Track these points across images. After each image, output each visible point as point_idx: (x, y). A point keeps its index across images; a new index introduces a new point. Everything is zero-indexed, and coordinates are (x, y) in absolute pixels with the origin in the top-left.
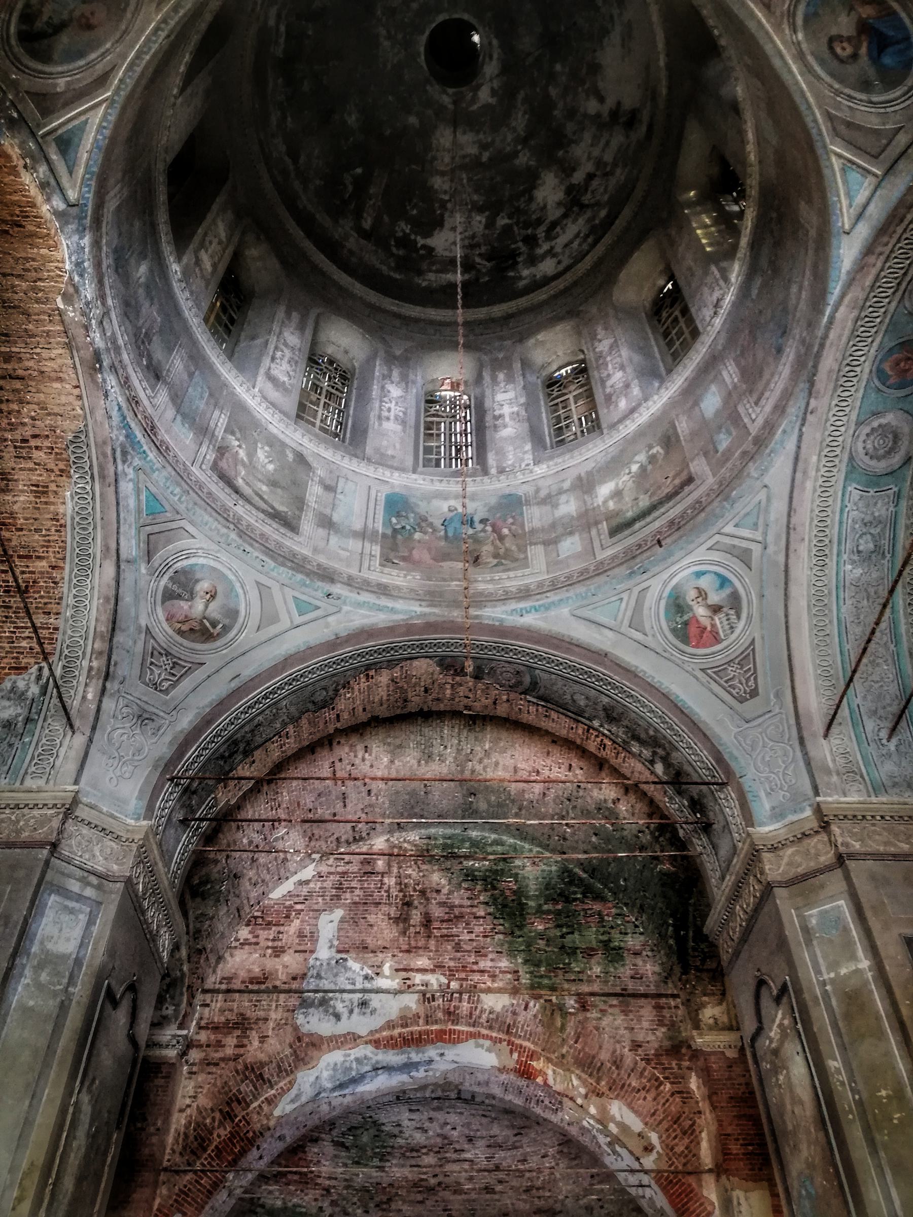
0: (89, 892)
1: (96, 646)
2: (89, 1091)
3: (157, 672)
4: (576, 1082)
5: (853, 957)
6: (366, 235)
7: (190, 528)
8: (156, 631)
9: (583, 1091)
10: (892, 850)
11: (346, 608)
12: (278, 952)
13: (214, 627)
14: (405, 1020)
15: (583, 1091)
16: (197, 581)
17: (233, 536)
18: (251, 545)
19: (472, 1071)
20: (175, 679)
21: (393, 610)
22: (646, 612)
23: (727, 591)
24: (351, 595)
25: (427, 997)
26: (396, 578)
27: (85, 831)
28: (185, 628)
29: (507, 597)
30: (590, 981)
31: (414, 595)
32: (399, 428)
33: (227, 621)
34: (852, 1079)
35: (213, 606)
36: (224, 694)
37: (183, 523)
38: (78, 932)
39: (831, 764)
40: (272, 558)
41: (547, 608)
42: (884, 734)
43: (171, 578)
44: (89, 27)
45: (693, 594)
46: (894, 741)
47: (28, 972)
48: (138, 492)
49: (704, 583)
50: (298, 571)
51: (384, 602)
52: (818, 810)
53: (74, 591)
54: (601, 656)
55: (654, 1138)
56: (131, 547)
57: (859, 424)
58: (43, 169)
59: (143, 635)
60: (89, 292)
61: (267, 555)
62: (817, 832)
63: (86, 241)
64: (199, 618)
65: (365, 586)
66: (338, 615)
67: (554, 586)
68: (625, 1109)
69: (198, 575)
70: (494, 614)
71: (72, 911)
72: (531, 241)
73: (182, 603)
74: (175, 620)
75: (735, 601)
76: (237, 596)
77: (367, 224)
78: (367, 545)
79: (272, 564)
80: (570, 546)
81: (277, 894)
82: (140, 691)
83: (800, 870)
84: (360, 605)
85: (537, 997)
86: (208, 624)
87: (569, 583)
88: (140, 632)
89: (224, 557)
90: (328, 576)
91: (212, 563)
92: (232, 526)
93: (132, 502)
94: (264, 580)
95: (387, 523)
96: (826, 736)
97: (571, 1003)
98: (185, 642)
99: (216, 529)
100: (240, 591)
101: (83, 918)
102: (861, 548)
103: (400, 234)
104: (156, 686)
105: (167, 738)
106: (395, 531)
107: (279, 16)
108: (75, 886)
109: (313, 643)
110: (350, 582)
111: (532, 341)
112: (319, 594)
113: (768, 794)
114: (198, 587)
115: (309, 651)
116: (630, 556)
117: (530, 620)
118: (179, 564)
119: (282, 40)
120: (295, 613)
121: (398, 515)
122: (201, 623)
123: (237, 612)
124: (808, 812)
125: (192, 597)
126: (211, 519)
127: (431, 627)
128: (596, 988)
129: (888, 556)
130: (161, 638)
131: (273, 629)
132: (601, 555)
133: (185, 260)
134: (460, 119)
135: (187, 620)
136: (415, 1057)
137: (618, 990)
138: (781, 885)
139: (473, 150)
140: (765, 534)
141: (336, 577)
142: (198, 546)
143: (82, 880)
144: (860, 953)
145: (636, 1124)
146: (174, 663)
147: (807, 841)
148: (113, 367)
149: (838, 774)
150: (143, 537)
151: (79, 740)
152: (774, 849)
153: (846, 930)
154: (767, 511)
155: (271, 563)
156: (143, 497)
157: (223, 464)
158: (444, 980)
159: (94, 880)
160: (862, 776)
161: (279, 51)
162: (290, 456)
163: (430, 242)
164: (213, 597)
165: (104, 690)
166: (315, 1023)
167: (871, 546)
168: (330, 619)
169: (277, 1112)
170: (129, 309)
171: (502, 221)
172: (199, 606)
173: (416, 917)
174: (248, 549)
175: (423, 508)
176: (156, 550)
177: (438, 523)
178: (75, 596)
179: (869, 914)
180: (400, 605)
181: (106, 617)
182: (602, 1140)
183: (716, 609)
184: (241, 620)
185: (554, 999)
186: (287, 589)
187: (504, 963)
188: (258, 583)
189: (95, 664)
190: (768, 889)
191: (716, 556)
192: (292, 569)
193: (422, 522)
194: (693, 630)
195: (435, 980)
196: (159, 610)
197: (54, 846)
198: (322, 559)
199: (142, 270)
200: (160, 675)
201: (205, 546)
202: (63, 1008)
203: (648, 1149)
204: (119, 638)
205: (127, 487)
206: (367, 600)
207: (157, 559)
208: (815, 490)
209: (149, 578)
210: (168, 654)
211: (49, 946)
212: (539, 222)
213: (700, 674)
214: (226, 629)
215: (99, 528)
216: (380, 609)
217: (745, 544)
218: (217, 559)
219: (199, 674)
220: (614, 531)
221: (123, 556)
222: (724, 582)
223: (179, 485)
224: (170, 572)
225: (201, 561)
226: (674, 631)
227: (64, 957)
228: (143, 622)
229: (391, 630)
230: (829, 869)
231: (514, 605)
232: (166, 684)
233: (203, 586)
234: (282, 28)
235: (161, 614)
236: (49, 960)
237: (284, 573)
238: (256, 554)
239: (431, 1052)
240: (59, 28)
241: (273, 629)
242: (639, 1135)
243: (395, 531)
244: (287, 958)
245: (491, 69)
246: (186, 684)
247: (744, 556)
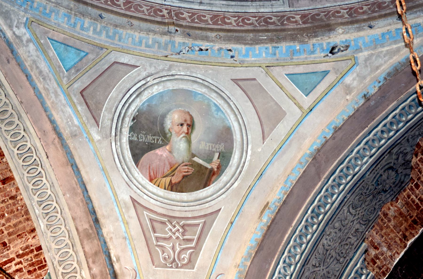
1: (87, 249)
3: (168, 246)
7: (125, 59)
8: (145, 200)
11: (362, 56)
13: (209, 160)
16: (164, 116)
17: (179, 39)
18: (206, 39)
20: (193, 245)
24: (362, 33)
28: (176, 179)
33: (221, 147)
35: (195, 136)
36: (259, 235)
37: (113, 57)
40: (239, 40)
43: (132, 129)
50: (279, 40)
53: (36, 198)
59: (132, 212)
61: (229, 40)
64: (186, 158)
66: (357, 69)
69: (161, 110)
73: (159, 151)
74: (160, 175)
76: (218, 109)
79: (242, 48)
84: (376, 43)
86: (201, 162)
88: (128, 209)
89: (180, 71)
91: (170, 86)
92: (172, 28)
98: (184, 196)
99: (155, 42)
100: (220, 102)
104: (174, 263)
109: (339, 122)
112: (319, 55)
114: (168, 124)
115: (340, 134)
118: (133, 108)
120: (299, 94)
122: (193, 164)
123: (228, 130)
125: (165, 138)
126: (143, 35)
130: (152, 204)
131: (282, 129)
141: (333, 21)
142: (144, 74)
146: (183, 227)
150: (76, 99)
164: (191, 126)
168: (348, 79)
172: (179, 146)
174: (204, 45)
176: (99, 105)
178: (40, 203)
181: (80, 212)
184: (237, 137)
186: (276, 71)
188: (235, 81)
189: (96, 270)
192: (271, 40)
196: (136, 173)
200: (173, 248)
201: (152, 70)
204: (108, 229)
206: (385, 30)
207: (105, 116)
209: (106, 143)
210: (171, 218)
214: (225, 157)
215: (24, 115)
218: (173, 78)
219: (219, 225)
221: (66, 133)
223: (83, 14)
224: (128, 122)
225: (156, 90)
232: (186, 256)
233: (172, 120)
235: (141, 178)
238: (217, 46)
246: (209, 244)
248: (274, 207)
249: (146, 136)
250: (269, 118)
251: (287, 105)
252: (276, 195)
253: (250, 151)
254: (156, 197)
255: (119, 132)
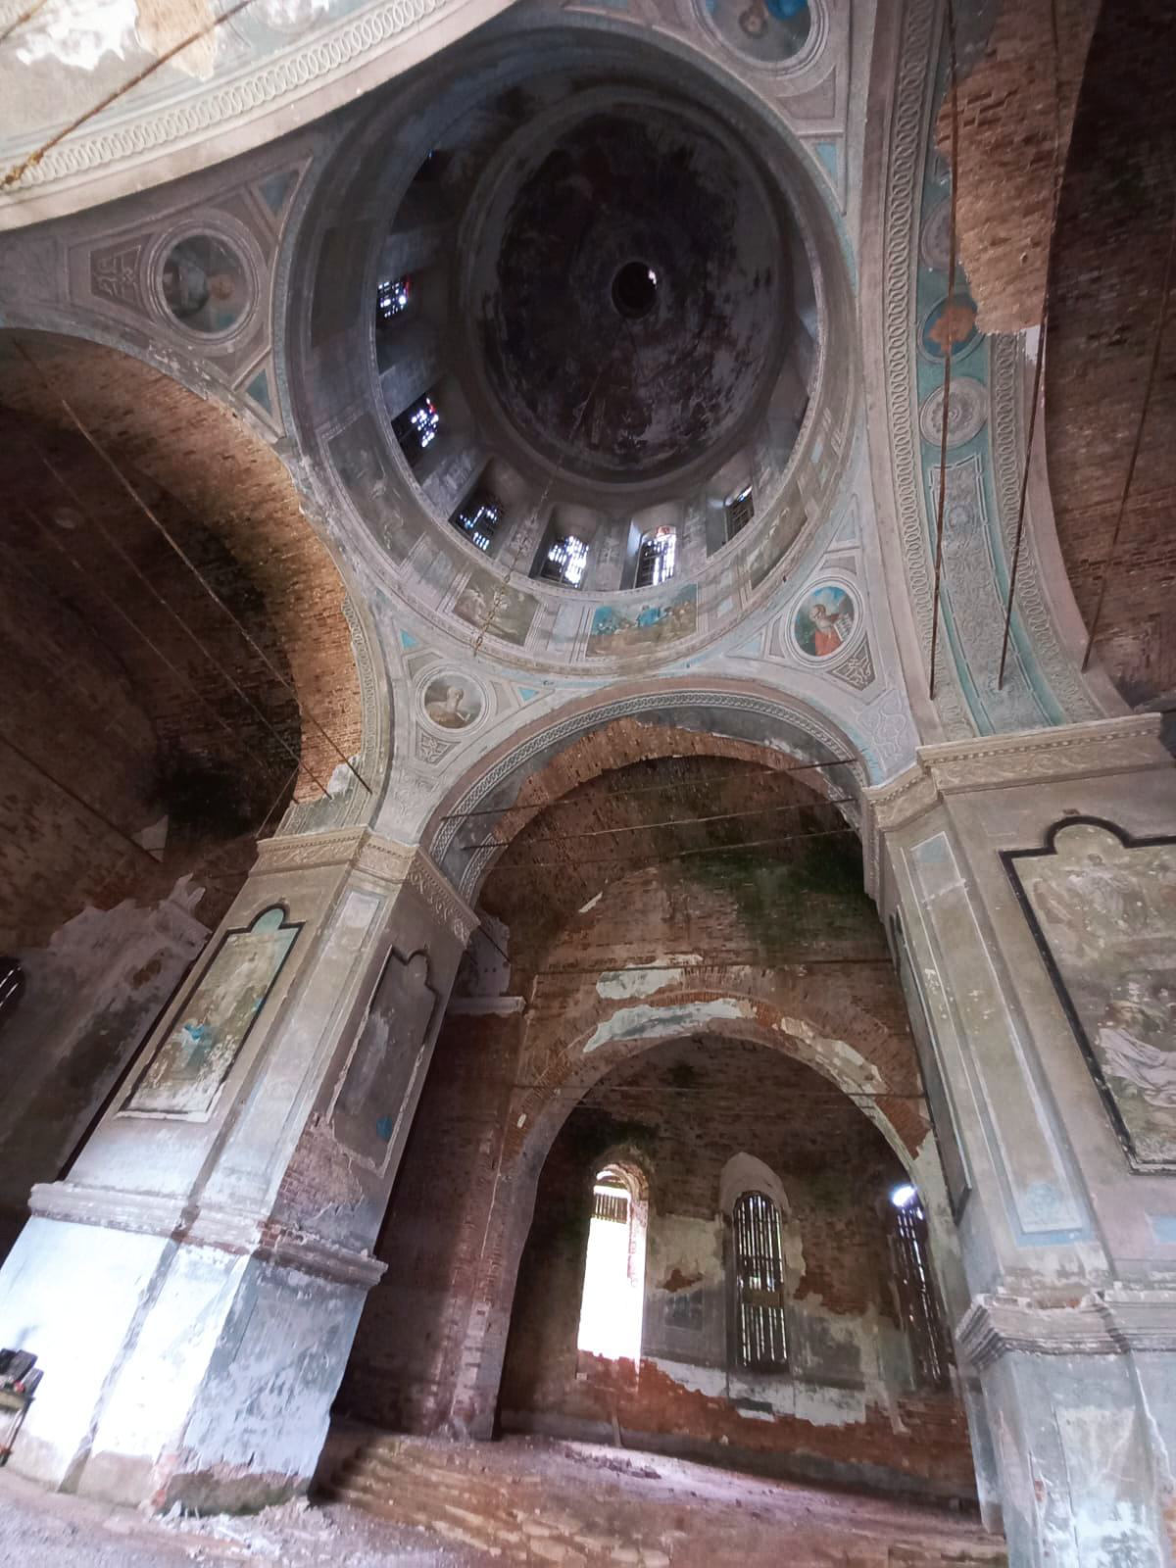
0: (378, 890)
2: (383, 1015)
4: (805, 1027)
5: (952, 879)
6: (595, 447)
9: (811, 1034)
10: (995, 780)
12: (586, 947)
14: (670, 988)
15: (811, 1034)
19: (724, 1022)
21: (593, 685)
22: (781, 638)
23: (842, 598)
25: (687, 969)
26: (598, 662)
27: (376, 853)
29: (680, 656)
30: (816, 953)
31: (609, 671)
32: (612, 565)
34: (947, 981)
37: (432, 650)
38: (370, 916)
39: (937, 719)
41: (707, 656)
42: (995, 684)
44: (224, 296)
45: (815, 611)
46: (1006, 688)
47: (333, 938)
48: (394, 632)
49: (821, 600)
51: (587, 680)
52: (921, 762)
54: (752, 683)
55: (874, 1070)
56: (397, 670)
57: (921, 403)
58: (248, 413)
60: (320, 498)
62: (922, 779)
63: (305, 461)
65: (574, 671)
67: (712, 639)
68: (847, 1047)
70: (665, 671)
71: (367, 902)
72: (715, 408)
75: (847, 606)
77: (595, 440)
78: (578, 645)
80: (726, 607)
81: (584, 910)
82: (414, 762)
83: (908, 814)
84: (570, 685)
85: (772, 967)
87: (723, 633)
90: (543, 669)
91: (458, 674)
93: (392, 641)
94: (496, 680)
95: (596, 626)
96: (932, 696)
97: (801, 970)
101: (374, 906)
102: (954, 522)
103: (620, 439)
105: (439, 793)
106: (601, 632)
107: (496, 313)
108: (368, 887)
110: (561, 671)
111: (715, 477)
113: (886, 759)
116: (765, 597)
117: (695, 669)
119: (504, 328)
121: (604, 621)
124: (914, 763)
125: (445, 698)
127: (624, 690)
128: (820, 958)
129: (984, 523)
130: (427, 728)
131: (508, 712)
132: (746, 605)
133: (428, 482)
134: (654, 338)
135: (445, 714)
136: (679, 1012)
137: (840, 958)
138: (891, 829)
139: (663, 358)
140: (861, 537)
143: (375, 884)
144: (958, 873)
145: (858, 1059)
147: (914, 789)
148: (356, 549)
149: (944, 726)
150: (405, 663)
151: (375, 797)
152: (886, 803)
153: (946, 856)
154: (859, 518)
155: (500, 668)
156: (399, 635)
157: (464, 608)
158: (700, 959)
159: (383, 883)
160: (969, 724)
161: (504, 335)
162: (522, 598)
163: (643, 437)
164: (461, 696)
165: (389, 767)
166: (607, 990)
167: (964, 518)
168: (548, 699)
169: (585, 1050)
170: (369, 514)
171: (693, 402)
173: (679, 917)
175: (623, 612)
177: (634, 620)
179: (963, 838)
180: (599, 680)
182: (834, 1073)
183: (834, 618)
185: (786, 968)
187: (746, 945)
190: (882, 835)
191: (828, 573)
193: (622, 622)
194: (818, 642)
195: (694, 959)
197: (353, 863)
198: (541, 660)
199: (379, 486)
202: (357, 960)
203: (870, 1078)
205: (386, 630)
207: (417, 675)
208: (894, 482)
210: (433, 738)
211: (350, 923)
212: (719, 392)
213: (827, 676)
214: (473, 717)
216: (580, 685)
217: (846, 554)
219: (456, 750)
220: (754, 586)
221: (393, 675)
222: (837, 591)
224: (429, 684)
226: (804, 647)
227: (359, 930)
228: (414, 719)
229: (591, 699)
230: (933, 807)
231: (682, 661)
234: (502, 317)
236: (352, 932)
237: (511, 673)
239: (691, 1008)
240: (203, 301)
241: (508, 712)
242: (861, 1067)
243: (601, 632)
244: (591, 950)
245: (664, 296)
247: (849, 565)
248: (489, 749)
249: (436, 692)
250: (502, 704)
251: (513, 702)
252: (492, 745)
253: (486, 718)
254: (429, 724)
255: (422, 687)
